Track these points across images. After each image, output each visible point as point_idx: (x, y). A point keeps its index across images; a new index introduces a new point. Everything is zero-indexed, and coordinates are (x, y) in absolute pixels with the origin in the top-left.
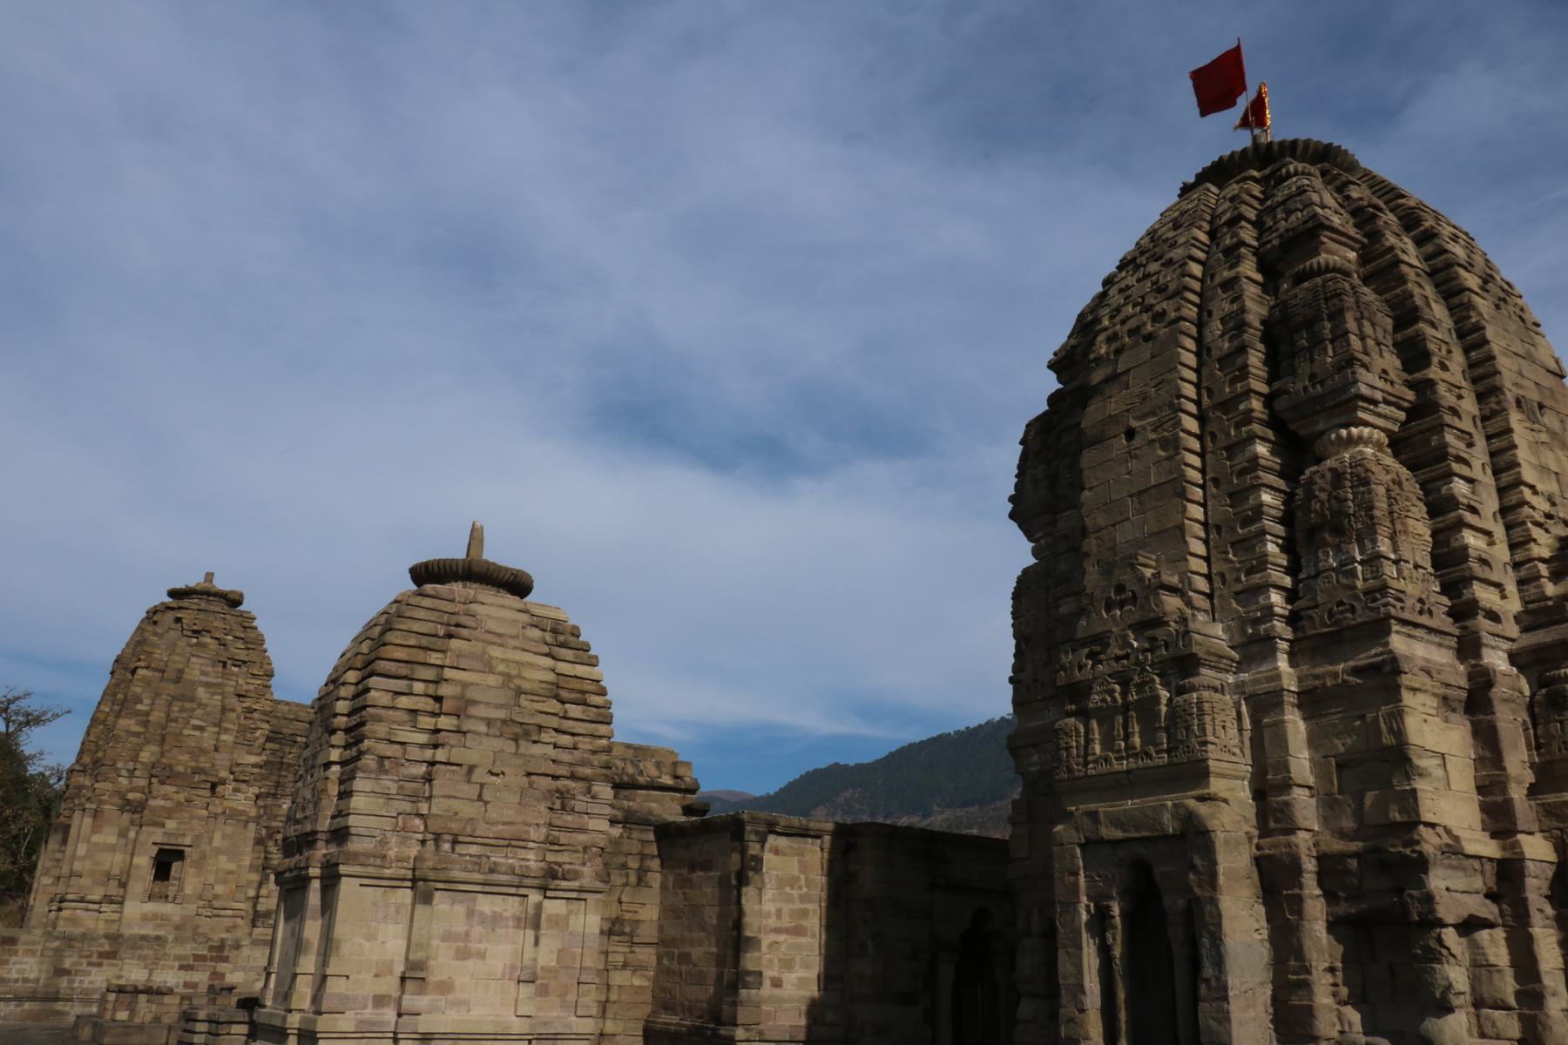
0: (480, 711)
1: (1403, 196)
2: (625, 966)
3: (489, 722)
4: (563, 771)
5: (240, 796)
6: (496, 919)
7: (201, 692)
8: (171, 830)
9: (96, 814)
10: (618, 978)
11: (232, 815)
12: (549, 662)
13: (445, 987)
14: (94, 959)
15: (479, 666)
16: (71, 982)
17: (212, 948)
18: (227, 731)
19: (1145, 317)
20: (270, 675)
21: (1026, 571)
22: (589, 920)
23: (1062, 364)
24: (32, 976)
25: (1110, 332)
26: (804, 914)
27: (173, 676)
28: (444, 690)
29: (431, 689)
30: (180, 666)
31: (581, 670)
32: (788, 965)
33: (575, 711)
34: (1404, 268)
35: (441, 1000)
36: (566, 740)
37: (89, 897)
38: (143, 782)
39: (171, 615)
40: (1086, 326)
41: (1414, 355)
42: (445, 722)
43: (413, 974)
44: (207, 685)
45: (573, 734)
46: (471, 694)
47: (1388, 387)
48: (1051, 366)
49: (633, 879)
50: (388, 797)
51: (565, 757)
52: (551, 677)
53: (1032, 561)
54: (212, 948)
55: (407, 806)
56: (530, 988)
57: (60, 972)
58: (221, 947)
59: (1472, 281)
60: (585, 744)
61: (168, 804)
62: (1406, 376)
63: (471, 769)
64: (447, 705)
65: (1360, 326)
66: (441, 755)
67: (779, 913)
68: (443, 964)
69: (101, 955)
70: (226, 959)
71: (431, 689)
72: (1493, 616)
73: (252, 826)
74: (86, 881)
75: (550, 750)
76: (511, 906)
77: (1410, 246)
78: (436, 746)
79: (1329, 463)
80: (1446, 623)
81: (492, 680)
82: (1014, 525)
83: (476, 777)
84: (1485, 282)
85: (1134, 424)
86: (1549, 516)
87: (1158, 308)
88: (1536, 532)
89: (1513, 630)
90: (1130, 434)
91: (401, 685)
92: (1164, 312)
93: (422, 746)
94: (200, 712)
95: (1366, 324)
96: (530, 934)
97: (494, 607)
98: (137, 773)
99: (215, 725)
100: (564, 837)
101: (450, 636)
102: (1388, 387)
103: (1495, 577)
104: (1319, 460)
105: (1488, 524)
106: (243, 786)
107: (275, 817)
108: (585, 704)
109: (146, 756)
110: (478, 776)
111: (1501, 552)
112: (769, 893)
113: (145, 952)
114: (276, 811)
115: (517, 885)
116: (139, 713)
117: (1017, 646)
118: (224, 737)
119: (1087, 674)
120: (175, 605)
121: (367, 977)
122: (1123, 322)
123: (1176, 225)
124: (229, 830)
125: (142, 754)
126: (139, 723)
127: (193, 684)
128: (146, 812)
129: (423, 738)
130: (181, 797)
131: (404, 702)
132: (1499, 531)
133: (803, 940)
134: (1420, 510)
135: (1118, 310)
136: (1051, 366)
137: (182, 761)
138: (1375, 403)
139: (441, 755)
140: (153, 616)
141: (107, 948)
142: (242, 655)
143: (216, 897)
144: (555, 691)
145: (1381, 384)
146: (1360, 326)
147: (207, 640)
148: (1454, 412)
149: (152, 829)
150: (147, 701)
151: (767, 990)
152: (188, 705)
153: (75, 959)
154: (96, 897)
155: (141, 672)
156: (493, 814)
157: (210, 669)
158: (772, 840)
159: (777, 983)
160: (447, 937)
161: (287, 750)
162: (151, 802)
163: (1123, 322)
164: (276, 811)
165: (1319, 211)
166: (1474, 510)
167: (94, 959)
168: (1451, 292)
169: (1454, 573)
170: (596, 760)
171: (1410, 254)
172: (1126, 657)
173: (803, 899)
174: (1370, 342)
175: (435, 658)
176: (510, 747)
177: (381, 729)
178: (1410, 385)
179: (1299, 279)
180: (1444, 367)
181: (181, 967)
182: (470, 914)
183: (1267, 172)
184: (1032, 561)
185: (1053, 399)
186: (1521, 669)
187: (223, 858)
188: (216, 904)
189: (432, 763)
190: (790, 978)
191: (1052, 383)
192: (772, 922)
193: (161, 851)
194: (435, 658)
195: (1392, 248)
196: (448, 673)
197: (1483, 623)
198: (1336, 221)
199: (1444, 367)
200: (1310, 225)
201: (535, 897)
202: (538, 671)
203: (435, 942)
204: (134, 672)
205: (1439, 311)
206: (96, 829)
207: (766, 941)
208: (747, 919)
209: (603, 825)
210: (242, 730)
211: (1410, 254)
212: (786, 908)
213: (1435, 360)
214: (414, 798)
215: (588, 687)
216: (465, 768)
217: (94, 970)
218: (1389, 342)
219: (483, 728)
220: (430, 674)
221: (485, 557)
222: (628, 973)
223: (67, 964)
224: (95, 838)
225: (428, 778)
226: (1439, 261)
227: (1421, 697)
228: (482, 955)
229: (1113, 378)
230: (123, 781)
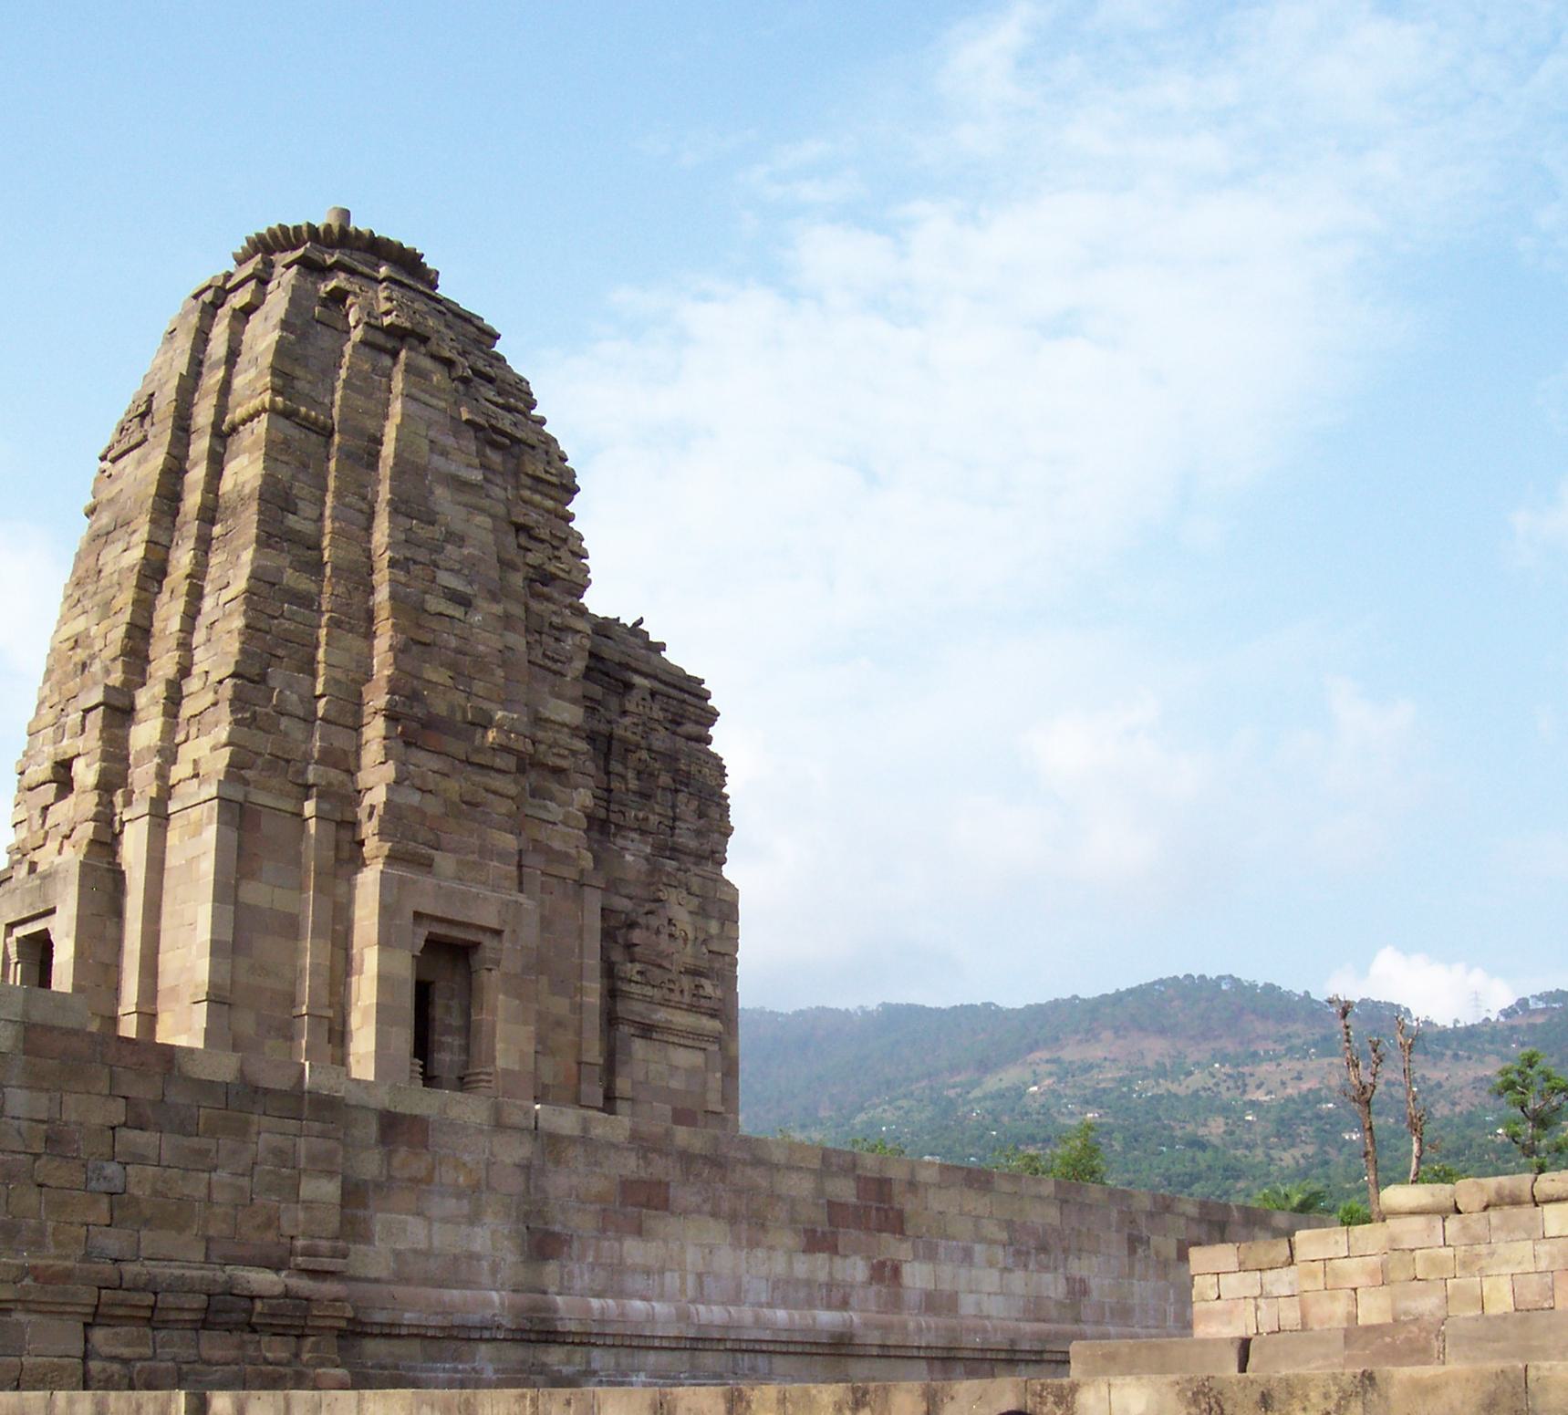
130: (453, 787)
157: (450, 442)
181: (816, 1242)
193: (433, 944)
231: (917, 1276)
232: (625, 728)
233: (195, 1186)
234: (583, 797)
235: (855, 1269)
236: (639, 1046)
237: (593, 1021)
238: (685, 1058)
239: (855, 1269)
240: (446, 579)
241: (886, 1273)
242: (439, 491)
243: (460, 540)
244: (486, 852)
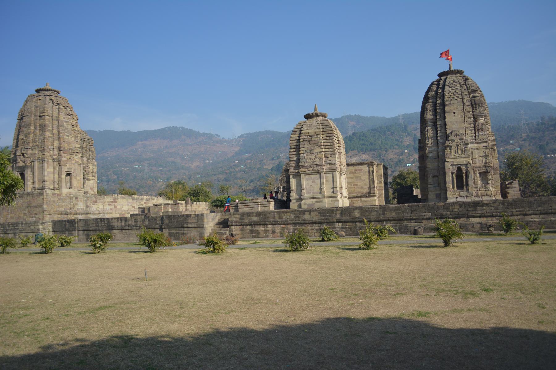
5: (77, 157)
57: (87, 207)
70: (116, 202)
73: (82, 166)
90: (454, 113)
98: (55, 150)
116: (49, 130)
126: (51, 134)
150: (51, 127)
181: (109, 205)
206: (48, 167)
230: (51, 152)
231: (118, 207)
232: (84, 146)
234: (80, 155)
235: (112, 207)
237: (82, 179)
238: (91, 182)
239: (112, 207)
240: (66, 134)
241: (115, 207)
242: (65, 123)
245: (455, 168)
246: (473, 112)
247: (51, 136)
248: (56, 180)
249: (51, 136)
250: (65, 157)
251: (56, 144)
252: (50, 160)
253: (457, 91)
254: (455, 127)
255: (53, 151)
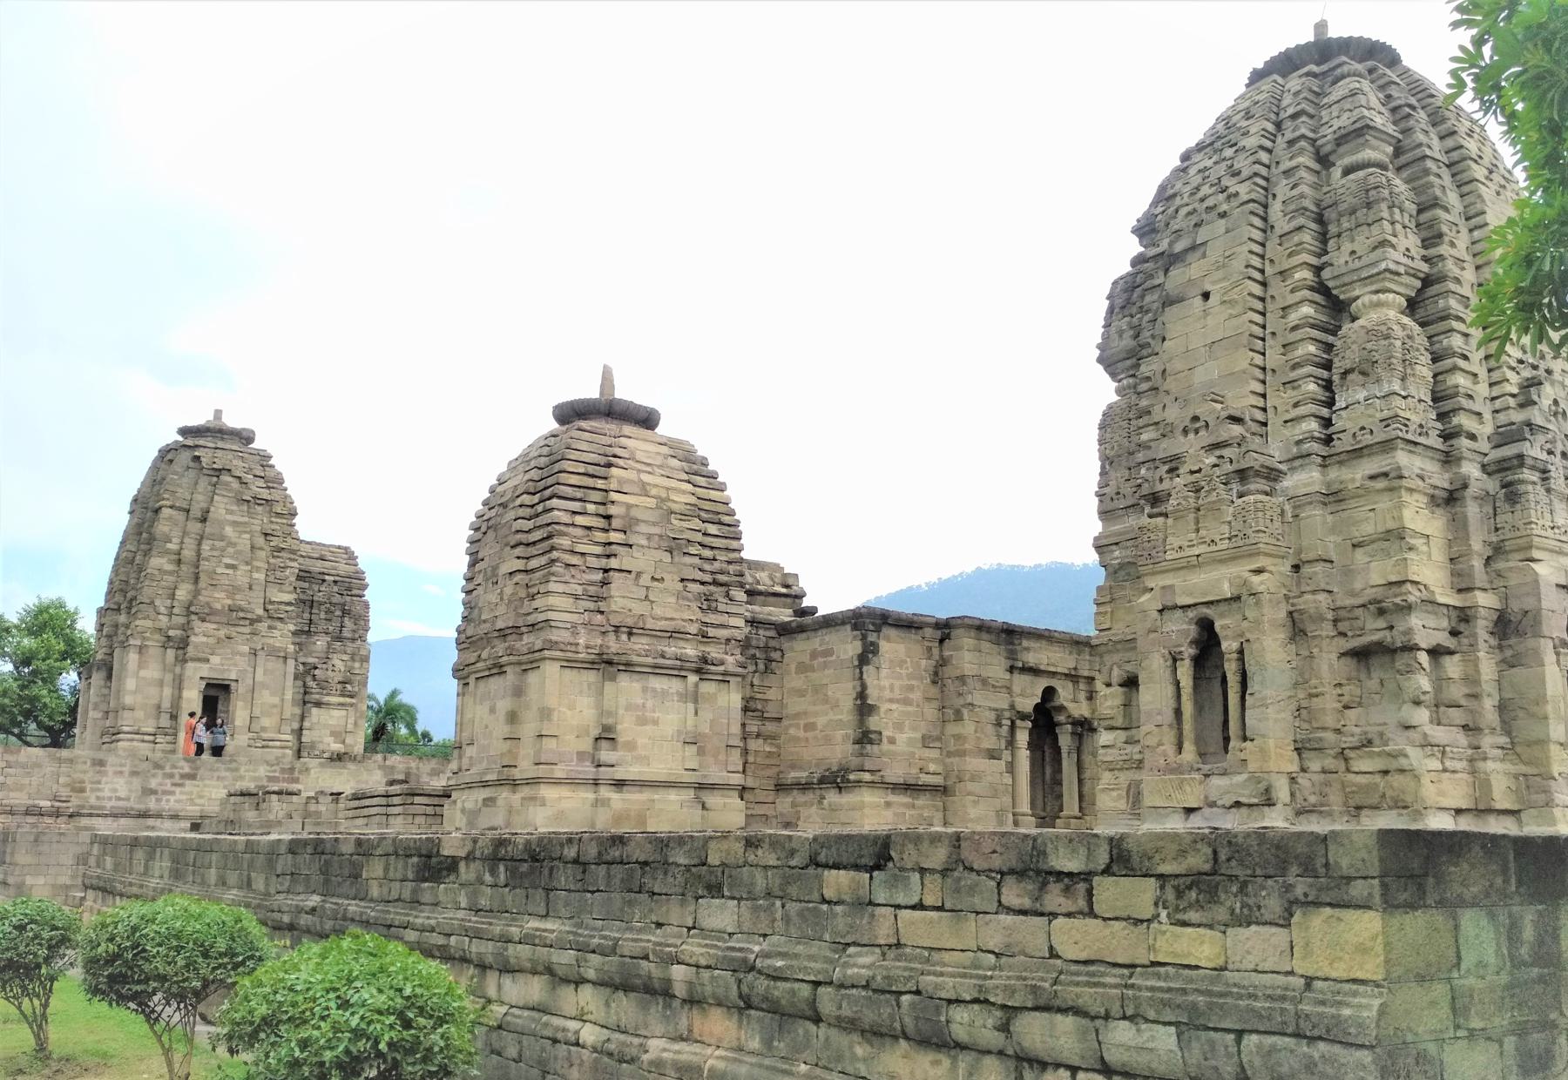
0: (643, 528)
1: (1433, 96)
2: (758, 736)
3: (649, 537)
4: (708, 578)
5: (276, 633)
6: (664, 693)
7: (229, 530)
8: (219, 666)
9: (141, 649)
10: (754, 745)
11: (273, 652)
12: (689, 487)
13: (631, 746)
14: (177, 780)
15: (637, 490)
16: (158, 800)
17: (283, 771)
18: (258, 569)
19: (1221, 197)
20: (293, 514)
21: (1110, 407)
22: (732, 698)
23: (1146, 229)
24: (122, 794)
25: (1190, 208)
26: (911, 688)
27: (199, 515)
28: (612, 510)
29: (601, 509)
30: (204, 505)
31: (714, 494)
32: (899, 727)
33: (713, 529)
34: (1429, 164)
35: (629, 756)
36: (707, 553)
37: (144, 730)
38: (182, 620)
39: (185, 457)
40: (1165, 195)
41: (1431, 238)
42: (615, 537)
43: (606, 736)
44: (235, 524)
45: (712, 548)
46: (634, 513)
47: (1409, 262)
48: (1135, 231)
49: (761, 667)
50: (576, 597)
51: (707, 567)
52: (693, 500)
53: (1115, 398)
54: (283, 771)
55: (591, 605)
56: (694, 748)
58: (292, 769)
59: (1479, 172)
60: (722, 556)
61: (211, 641)
62: (1423, 252)
63: (639, 574)
64: (616, 523)
65: (1392, 214)
66: (614, 563)
67: (892, 688)
68: (626, 728)
69: (183, 776)
71: (601, 509)
72: (1473, 437)
73: (291, 663)
74: (139, 714)
75: (696, 560)
76: (675, 685)
77: (1435, 142)
78: (608, 556)
79: (1361, 322)
80: (1437, 443)
81: (651, 502)
82: (1100, 367)
83: (642, 582)
84: (1491, 172)
85: (1208, 287)
86: (1521, 362)
87: (1232, 190)
88: (1510, 375)
89: (1484, 446)
91: (576, 506)
92: (1237, 194)
93: (598, 556)
94: (231, 550)
95: (1396, 210)
96: (691, 706)
97: (634, 441)
98: (176, 611)
99: (247, 563)
100: (711, 632)
101: (609, 465)
102: (1409, 262)
103: (1477, 408)
104: (1354, 319)
105: (1474, 368)
106: (279, 625)
107: (310, 654)
108: (720, 523)
109: (183, 593)
110: (645, 580)
111: (1482, 389)
112: (884, 672)
113: (223, 774)
114: (313, 648)
115: (678, 669)
116: (168, 552)
117: (1103, 467)
118: (256, 575)
119: (1166, 485)
120: (190, 442)
121: (571, 737)
122: (1202, 200)
123: (1248, 115)
124: (270, 665)
125: (178, 593)
126: (170, 562)
127: (221, 524)
128: (190, 649)
129: (598, 550)
130: (222, 633)
131: (579, 520)
132: (1483, 373)
133: (910, 709)
134: (1426, 358)
135: (1198, 189)
136: (1134, 231)
137: (220, 600)
138: (1398, 274)
139: (614, 563)
140: (167, 455)
141: (187, 770)
142: (265, 494)
143: (264, 729)
144: (694, 512)
145: (1404, 260)
146: (1392, 214)
147: (225, 478)
148: (1458, 281)
149: (198, 665)
151: (885, 746)
152: (218, 544)
153: (159, 779)
154: (151, 730)
155: (166, 512)
156: (658, 611)
157: (235, 508)
158: (886, 631)
159: (892, 741)
160: (628, 708)
161: (316, 588)
162: (193, 639)
163: (1202, 200)
164: (313, 648)
165: (1366, 113)
166: (1465, 358)
167: (177, 780)
168: (1464, 185)
169: (1447, 406)
170: (731, 568)
171: (1436, 148)
172: (1199, 471)
173: (910, 677)
174: (1398, 227)
175: (600, 484)
176: (667, 557)
177: (565, 542)
178: (1426, 259)
179: (1348, 171)
180: (1452, 245)
182: (645, 690)
183: (1324, 67)
184: (1115, 398)
185: (1138, 261)
186: (1489, 474)
187: (266, 693)
188: (265, 735)
189: (606, 571)
190: (902, 738)
191: (1135, 247)
192: (887, 694)
193: (208, 685)
194: (600, 484)
195: (1420, 145)
196: (614, 496)
197: (1464, 442)
198: (1379, 121)
199: (1452, 245)
200: (1358, 125)
201: (693, 678)
202: (682, 497)
203: (621, 712)
204: (157, 511)
205: (1452, 198)
206: (141, 666)
207: (884, 707)
208: (869, 691)
209: (740, 622)
210: (271, 569)
211: (1436, 148)
212: (897, 683)
213: (1446, 239)
214: (598, 598)
215: (720, 508)
216: (633, 575)
217: (178, 790)
218: (1413, 225)
219: (644, 542)
220: (596, 496)
221: (617, 396)
222: (761, 741)
223: (153, 784)
224: (143, 673)
225: (605, 583)
226: (1455, 155)
227: (1416, 496)
228: (655, 722)
229: (1193, 248)
230: (164, 619)
233: (26, 781)
236: (315, 711)
238: (336, 713)
243: (234, 545)
244: (235, 653)
245: (1181, 629)
246: (1318, 270)
247: (170, 567)
248: (166, 705)
249: (170, 567)
250: (203, 634)
251: (183, 593)
252: (154, 642)
253: (1242, 163)
254: (1207, 373)
255: (170, 615)
